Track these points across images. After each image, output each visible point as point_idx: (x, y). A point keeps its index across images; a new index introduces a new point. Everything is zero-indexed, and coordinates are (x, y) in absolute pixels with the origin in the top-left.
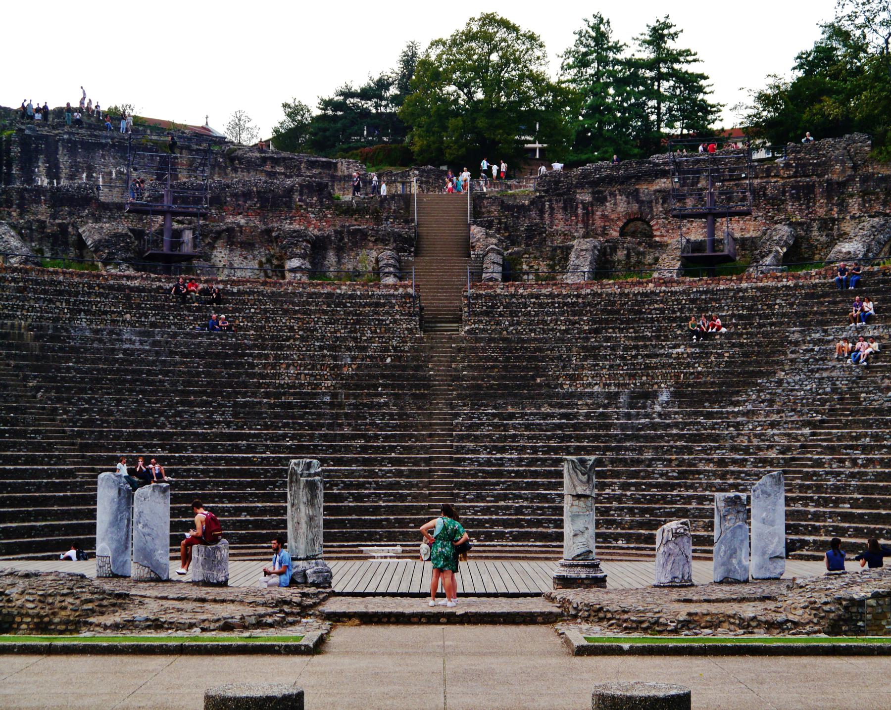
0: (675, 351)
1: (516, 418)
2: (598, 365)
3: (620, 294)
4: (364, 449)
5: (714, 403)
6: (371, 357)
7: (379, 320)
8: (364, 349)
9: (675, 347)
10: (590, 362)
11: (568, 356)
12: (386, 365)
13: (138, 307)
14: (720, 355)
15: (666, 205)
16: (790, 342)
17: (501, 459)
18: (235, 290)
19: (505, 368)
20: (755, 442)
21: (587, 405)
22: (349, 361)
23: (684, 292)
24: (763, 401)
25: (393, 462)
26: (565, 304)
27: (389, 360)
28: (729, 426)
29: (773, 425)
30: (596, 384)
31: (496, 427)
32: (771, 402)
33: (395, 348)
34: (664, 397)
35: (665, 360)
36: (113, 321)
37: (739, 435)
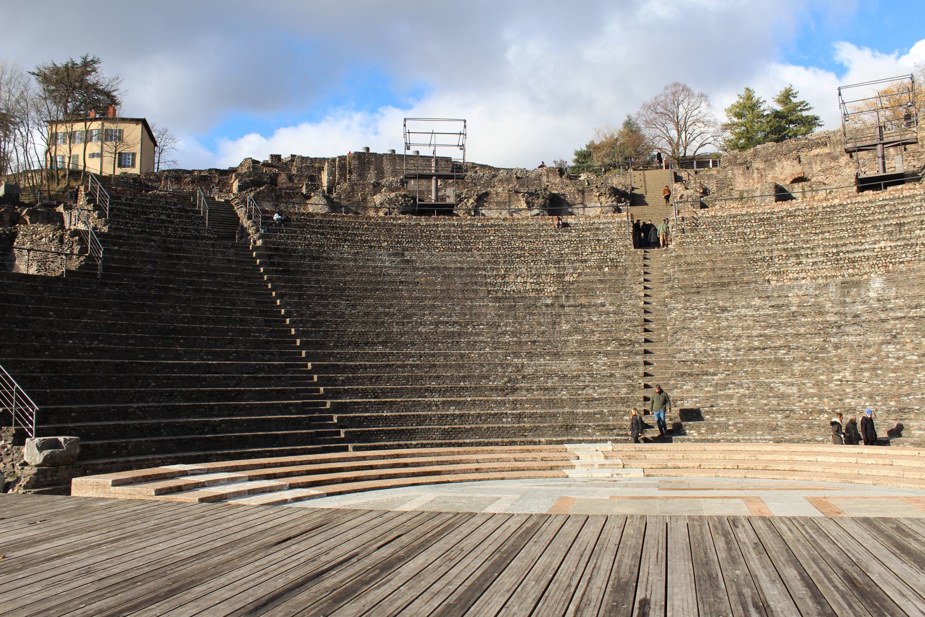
0: (876, 246)
1: (729, 311)
2: (801, 263)
3: (810, 209)
4: (580, 343)
6: (590, 267)
7: (598, 240)
8: (586, 261)
9: (875, 243)
10: (793, 260)
11: (771, 258)
12: (604, 273)
13: (397, 236)
15: (823, 166)
17: (717, 349)
18: (479, 224)
19: (713, 270)
21: (798, 296)
22: (571, 271)
23: (871, 202)
25: (606, 354)
26: (760, 220)
27: (606, 269)
30: (803, 278)
31: (709, 320)
33: (612, 260)
34: (877, 284)
35: (866, 254)
36: (371, 247)
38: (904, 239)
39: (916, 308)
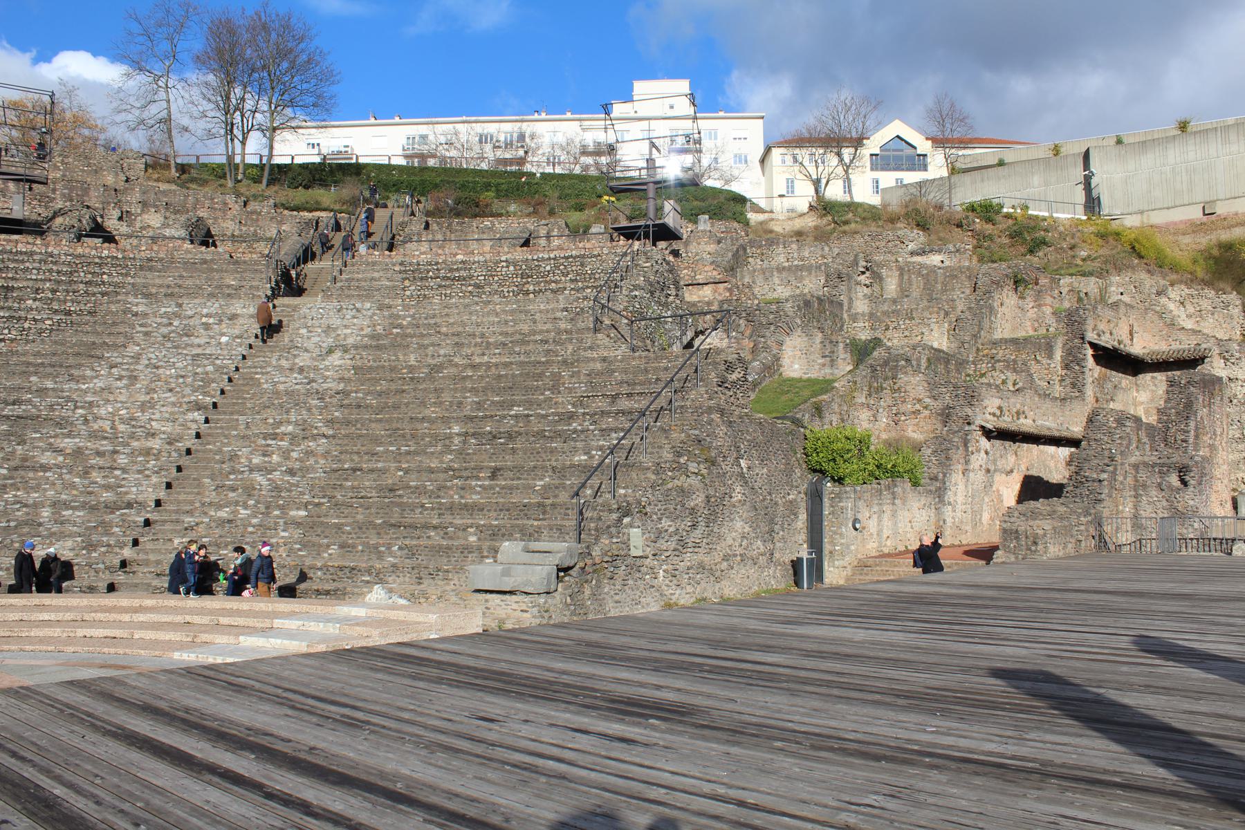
5: (47, 376)
14: (42, 320)
16: (136, 314)
20: (122, 427)
24: (120, 378)
28: (76, 407)
29: (143, 407)
32: (133, 379)
37: (96, 418)
38: (10, 308)
39: (14, 404)
